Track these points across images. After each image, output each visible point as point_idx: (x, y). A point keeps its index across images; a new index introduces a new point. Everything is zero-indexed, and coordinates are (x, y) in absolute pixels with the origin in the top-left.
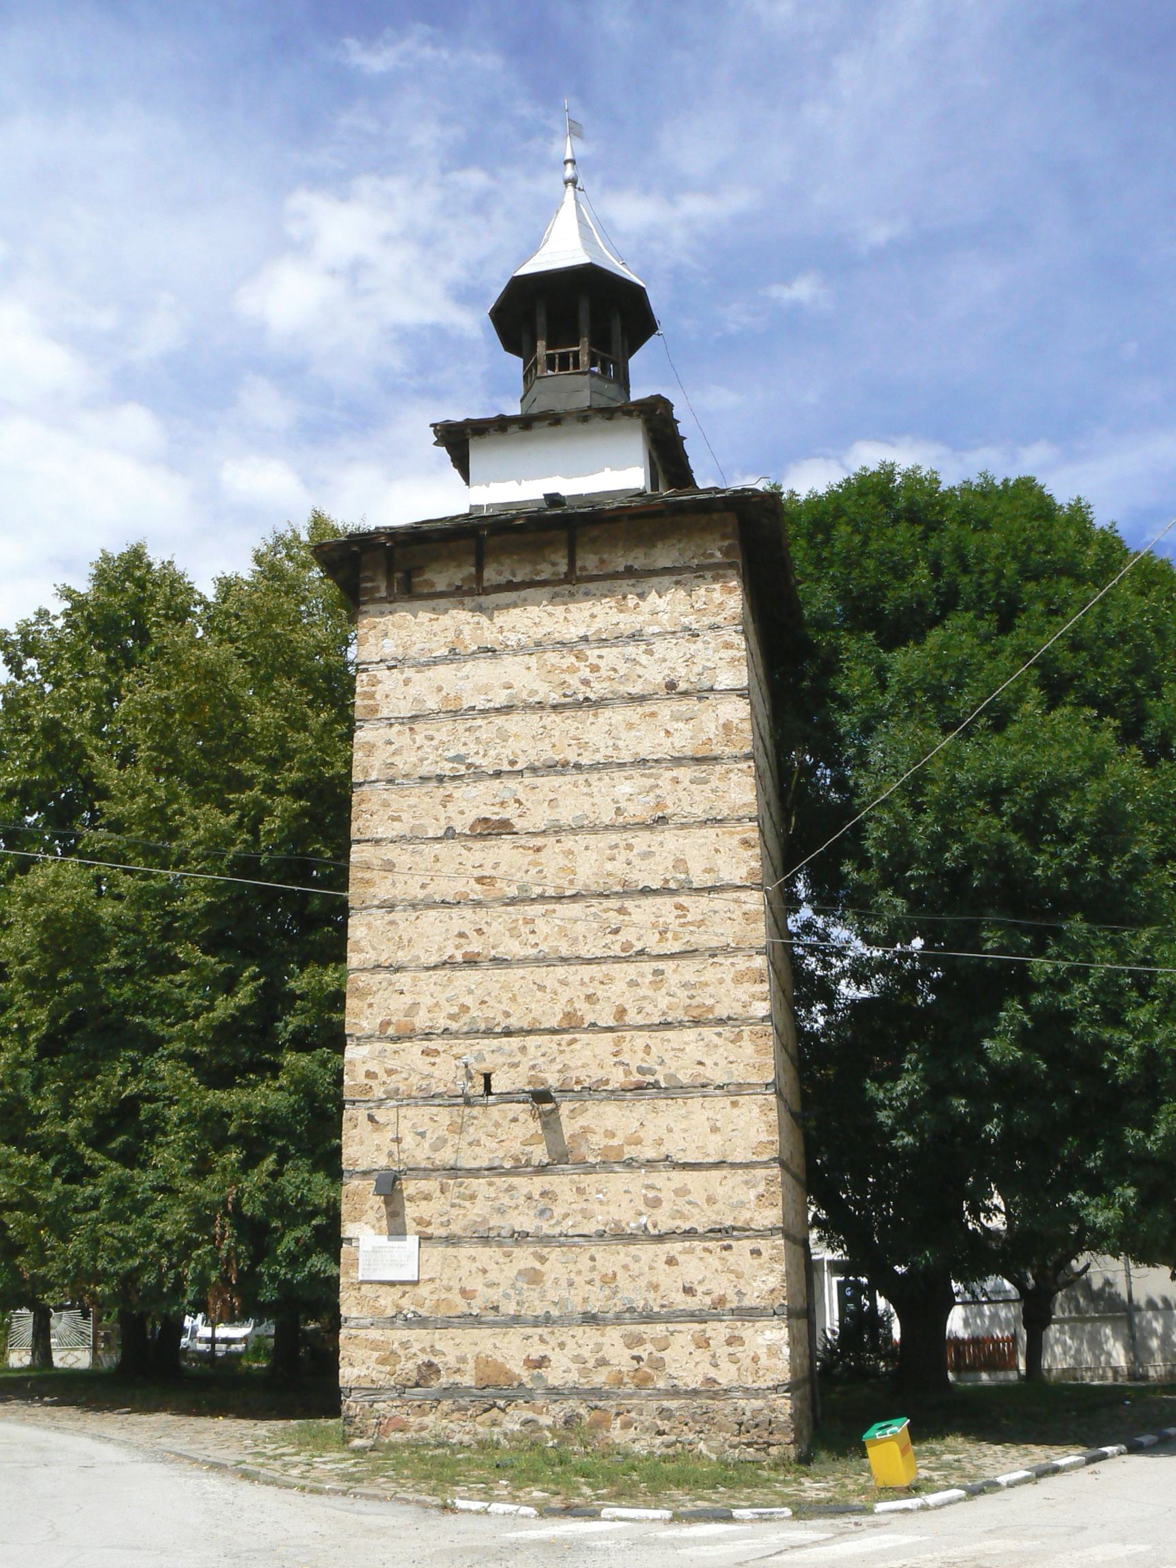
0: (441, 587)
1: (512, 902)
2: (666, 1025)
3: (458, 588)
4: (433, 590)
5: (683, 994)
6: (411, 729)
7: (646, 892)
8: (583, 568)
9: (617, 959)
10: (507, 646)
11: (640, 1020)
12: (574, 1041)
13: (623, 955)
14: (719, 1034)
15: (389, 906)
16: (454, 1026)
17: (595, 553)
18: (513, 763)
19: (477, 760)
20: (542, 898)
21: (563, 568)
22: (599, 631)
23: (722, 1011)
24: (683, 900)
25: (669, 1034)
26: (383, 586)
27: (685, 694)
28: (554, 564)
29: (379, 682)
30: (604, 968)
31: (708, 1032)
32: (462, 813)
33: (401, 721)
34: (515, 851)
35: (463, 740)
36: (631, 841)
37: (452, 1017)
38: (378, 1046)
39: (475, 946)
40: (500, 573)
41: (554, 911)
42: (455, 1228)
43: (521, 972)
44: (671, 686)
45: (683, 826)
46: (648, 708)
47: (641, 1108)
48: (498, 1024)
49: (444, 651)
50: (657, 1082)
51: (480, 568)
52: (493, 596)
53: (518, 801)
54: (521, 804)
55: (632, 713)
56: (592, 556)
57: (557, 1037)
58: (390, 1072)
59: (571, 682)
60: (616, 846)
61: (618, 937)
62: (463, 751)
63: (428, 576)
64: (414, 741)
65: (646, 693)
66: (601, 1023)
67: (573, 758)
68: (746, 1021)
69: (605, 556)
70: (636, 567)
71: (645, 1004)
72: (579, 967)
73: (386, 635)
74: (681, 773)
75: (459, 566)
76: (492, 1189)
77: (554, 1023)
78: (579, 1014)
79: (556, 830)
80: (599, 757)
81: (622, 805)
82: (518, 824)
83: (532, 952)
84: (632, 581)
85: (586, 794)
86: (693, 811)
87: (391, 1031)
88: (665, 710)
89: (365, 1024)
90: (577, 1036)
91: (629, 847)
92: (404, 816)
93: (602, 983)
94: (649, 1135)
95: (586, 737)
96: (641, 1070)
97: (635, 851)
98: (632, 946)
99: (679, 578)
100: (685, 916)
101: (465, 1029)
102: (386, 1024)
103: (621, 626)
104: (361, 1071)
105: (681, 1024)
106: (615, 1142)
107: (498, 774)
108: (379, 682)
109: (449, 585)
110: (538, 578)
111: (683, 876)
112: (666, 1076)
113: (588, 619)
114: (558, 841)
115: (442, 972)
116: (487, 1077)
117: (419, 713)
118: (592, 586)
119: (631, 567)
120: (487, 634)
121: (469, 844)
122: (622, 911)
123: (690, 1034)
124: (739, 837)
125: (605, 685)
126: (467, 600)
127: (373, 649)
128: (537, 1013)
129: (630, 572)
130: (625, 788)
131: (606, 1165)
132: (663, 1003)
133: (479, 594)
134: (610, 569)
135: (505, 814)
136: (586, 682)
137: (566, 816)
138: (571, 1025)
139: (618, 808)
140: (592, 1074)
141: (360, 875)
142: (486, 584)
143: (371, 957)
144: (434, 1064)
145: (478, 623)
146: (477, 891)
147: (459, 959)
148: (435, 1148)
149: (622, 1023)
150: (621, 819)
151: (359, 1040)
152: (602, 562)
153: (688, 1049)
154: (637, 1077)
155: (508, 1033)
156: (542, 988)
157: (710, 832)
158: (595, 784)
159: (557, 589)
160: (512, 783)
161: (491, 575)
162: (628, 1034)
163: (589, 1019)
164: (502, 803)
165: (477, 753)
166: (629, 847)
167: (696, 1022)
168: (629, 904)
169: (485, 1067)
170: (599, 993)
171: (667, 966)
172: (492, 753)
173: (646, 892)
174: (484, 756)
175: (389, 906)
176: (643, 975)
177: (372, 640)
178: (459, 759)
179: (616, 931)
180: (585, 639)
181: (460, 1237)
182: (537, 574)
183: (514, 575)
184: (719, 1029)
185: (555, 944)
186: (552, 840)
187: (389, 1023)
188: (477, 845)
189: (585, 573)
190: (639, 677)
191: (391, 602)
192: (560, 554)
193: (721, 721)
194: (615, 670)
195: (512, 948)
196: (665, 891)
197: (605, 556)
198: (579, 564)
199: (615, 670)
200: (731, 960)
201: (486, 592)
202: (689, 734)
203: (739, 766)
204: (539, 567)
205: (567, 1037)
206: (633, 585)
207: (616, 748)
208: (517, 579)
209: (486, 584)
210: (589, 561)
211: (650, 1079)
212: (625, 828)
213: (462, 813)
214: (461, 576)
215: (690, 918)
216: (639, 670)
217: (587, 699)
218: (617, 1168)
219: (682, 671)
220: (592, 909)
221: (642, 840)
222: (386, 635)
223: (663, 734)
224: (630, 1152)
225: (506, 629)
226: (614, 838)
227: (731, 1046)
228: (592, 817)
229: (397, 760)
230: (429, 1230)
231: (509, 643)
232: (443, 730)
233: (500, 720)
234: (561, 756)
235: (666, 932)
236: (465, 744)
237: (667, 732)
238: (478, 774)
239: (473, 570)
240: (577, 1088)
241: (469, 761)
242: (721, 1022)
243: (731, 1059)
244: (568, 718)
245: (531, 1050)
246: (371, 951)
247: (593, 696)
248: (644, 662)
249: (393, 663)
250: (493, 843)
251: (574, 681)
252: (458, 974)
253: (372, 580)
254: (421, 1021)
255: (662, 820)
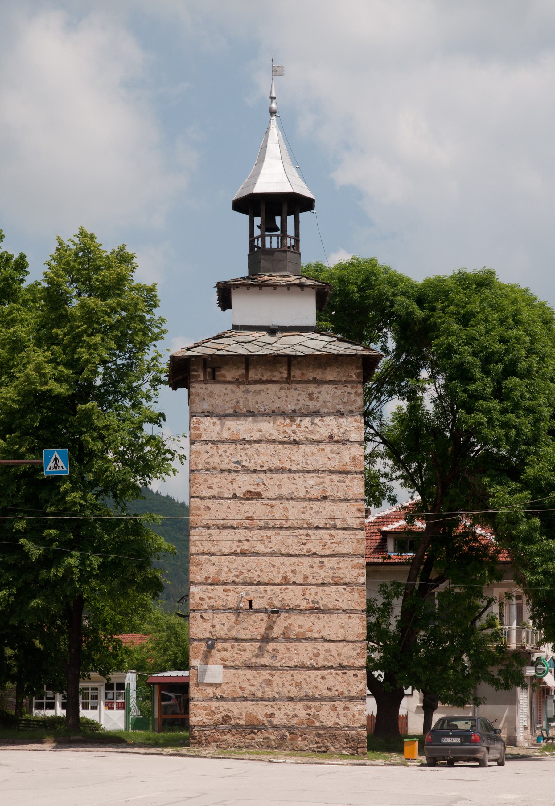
0: (229, 378)
1: (261, 528)
2: (323, 584)
3: (237, 380)
4: (225, 379)
5: (331, 572)
6: (217, 447)
7: (317, 528)
8: (294, 377)
9: (305, 556)
10: (259, 411)
11: (313, 581)
12: (287, 588)
13: (307, 554)
14: (345, 589)
15: (208, 527)
16: (237, 580)
17: (300, 369)
18: (262, 466)
19: (246, 464)
20: (274, 528)
21: (285, 375)
22: (301, 409)
23: (347, 580)
24: (333, 532)
25: (326, 588)
26: (202, 375)
27: (337, 442)
28: (281, 373)
29: (202, 423)
30: (300, 559)
31: (341, 588)
32: (240, 487)
33: (212, 442)
34: (262, 506)
35: (240, 454)
36: (312, 506)
37: (237, 576)
38: (205, 587)
39: (245, 546)
40: (256, 375)
41: (279, 533)
42: (237, 662)
43: (265, 558)
44: (331, 437)
45: (334, 501)
46: (321, 446)
47: (313, 617)
48: (255, 580)
49: (231, 411)
50: (320, 607)
51: (247, 370)
52: (253, 385)
53: (264, 484)
54: (265, 485)
55: (314, 448)
56: (298, 371)
57: (279, 587)
58: (210, 598)
59: (288, 431)
60: (306, 507)
61: (305, 546)
62: (240, 459)
63: (223, 372)
64: (218, 453)
65: (320, 439)
66: (297, 582)
67: (288, 467)
68: (356, 584)
69: (304, 372)
70: (317, 378)
71: (316, 575)
72: (289, 558)
73: (204, 399)
74: (335, 477)
75: (237, 368)
76: (252, 647)
77: (278, 581)
78: (289, 577)
79: (281, 498)
80: (299, 467)
81: (309, 490)
82: (264, 494)
83: (269, 550)
84: (316, 385)
85: (293, 483)
86: (338, 495)
87: (210, 581)
88: (328, 448)
89: (198, 577)
90: (287, 586)
91: (311, 508)
92: (214, 487)
93: (298, 565)
94: (315, 628)
95: (294, 458)
96: (313, 602)
97: (314, 510)
98: (311, 551)
99: (336, 386)
100: (333, 539)
101: (242, 581)
102: (207, 578)
103: (310, 407)
104: (197, 597)
105: (329, 584)
106: (302, 630)
107: (255, 471)
108: (202, 423)
109: (233, 378)
110: (274, 379)
111: (333, 523)
112: (323, 605)
113: (296, 402)
114: (281, 503)
115: (231, 557)
116: (250, 602)
117: (220, 439)
118: (298, 386)
119: (316, 378)
120: (250, 404)
121: (243, 501)
122: (308, 535)
123: (334, 588)
124: (356, 507)
125: (303, 434)
126: (241, 386)
127: (198, 406)
128: (271, 576)
129: (315, 381)
130: (311, 482)
131: (298, 640)
132: (323, 575)
133: (247, 384)
134: (305, 378)
135: (259, 489)
136: (294, 432)
137: (285, 492)
138: (286, 582)
139: (307, 491)
140: (293, 603)
141: (195, 512)
142: (250, 379)
143: (200, 549)
144: (228, 596)
145: (246, 398)
146: (246, 523)
147: (239, 552)
148: (229, 630)
149: (305, 582)
150: (308, 496)
151: (195, 584)
152: (303, 374)
153: (332, 595)
154: (311, 605)
155: (259, 584)
156: (274, 566)
157: (344, 504)
158: (297, 479)
159: (282, 385)
160: (262, 476)
161: (252, 375)
162: (308, 587)
163: (293, 580)
164: (257, 484)
165: (246, 461)
166: (311, 508)
167: (336, 584)
168: (310, 532)
169: (249, 598)
170: (297, 570)
171: (325, 560)
172: (253, 461)
173: (317, 528)
174: (249, 462)
175: (208, 527)
176: (315, 563)
177: (197, 401)
178: (238, 462)
179: (304, 544)
180: (294, 411)
181: (239, 666)
182: (274, 377)
183: (263, 376)
184: (345, 587)
185: (279, 547)
186: (278, 503)
187: (209, 578)
188: (246, 502)
189: (295, 379)
190: (318, 432)
191: (206, 383)
192: (284, 368)
193: (352, 455)
194: (307, 428)
195: (261, 548)
196: (325, 528)
197: (304, 372)
198: (292, 374)
199: (307, 428)
200: (351, 559)
201: (250, 383)
202: (338, 460)
203: (358, 476)
204: (274, 374)
205: (284, 587)
206: (316, 387)
207: (307, 463)
208: (264, 378)
209: (250, 379)
210: (297, 373)
211: (317, 606)
212: (310, 499)
213: (240, 487)
214: (238, 374)
215: (335, 541)
216: (318, 429)
217: (294, 440)
218: (303, 641)
219: (336, 431)
220: (295, 534)
221: (316, 506)
222: (204, 399)
223: (327, 459)
224: (308, 634)
225: (259, 402)
226: (305, 503)
227: (349, 594)
228: (296, 494)
229: (210, 460)
230: (227, 663)
231: (260, 410)
232: (230, 448)
233: (256, 446)
234: (283, 465)
235: (325, 545)
236: (241, 456)
237: (329, 458)
238: (246, 470)
239: (244, 371)
240: (287, 608)
241: (243, 464)
242: (345, 584)
243: (349, 599)
244: (286, 448)
245: (269, 592)
246: (201, 546)
247: (297, 439)
248: (320, 425)
249: (207, 414)
250: (253, 502)
251: (289, 432)
252: (239, 558)
253: (197, 371)
254: (223, 577)
255: (325, 498)
